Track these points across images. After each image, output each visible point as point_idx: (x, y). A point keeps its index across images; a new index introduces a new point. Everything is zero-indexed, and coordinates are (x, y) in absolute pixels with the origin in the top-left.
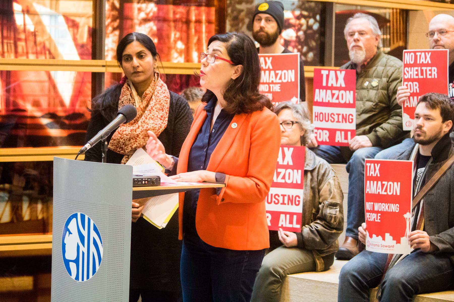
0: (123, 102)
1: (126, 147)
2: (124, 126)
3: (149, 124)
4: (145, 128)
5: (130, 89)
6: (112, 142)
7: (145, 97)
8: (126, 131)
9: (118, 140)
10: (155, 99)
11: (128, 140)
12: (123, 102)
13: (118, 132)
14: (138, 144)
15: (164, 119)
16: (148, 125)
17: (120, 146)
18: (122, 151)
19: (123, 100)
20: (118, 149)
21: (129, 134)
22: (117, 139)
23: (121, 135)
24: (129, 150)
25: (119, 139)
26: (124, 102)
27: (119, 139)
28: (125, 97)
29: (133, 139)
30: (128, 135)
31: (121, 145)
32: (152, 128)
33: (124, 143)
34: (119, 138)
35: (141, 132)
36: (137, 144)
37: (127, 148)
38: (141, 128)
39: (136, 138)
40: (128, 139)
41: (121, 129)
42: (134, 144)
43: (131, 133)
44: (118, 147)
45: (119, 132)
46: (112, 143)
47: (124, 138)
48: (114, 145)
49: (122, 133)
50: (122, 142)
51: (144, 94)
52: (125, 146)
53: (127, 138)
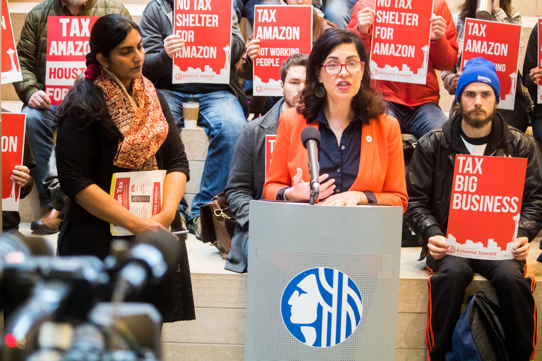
0: (115, 103)
1: (137, 160)
2: (130, 134)
3: (156, 128)
4: (155, 133)
5: (118, 87)
6: (122, 156)
7: (136, 94)
8: (136, 139)
9: (129, 152)
10: (150, 95)
11: (141, 150)
12: (115, 103)
13: (126, 142)
14: (152, 153)
15: (164, 119)
16: (156, 130)
17: (130, 159)
18: (132, 166)
19: (114, 101)
20: (127, 163)
21: (141, 142)
22: (128, 151)
23: (132, 145)
24: (143, 162)
25: (130, 151)
26: (116, 103)
27: (130, 151)
28: (116, 96)
29: (145, 149)
30: (140, 144)
31: (131, 158)
32: (161, 131)
33: (136, 154)
34: (130, 150)
35: (152, 138)
36: (151, 154)
37: (139, 160)
38: (150, 133)
39: (149, 146)
40: (140, 149)
41: (128, 138)
42: (148, 154)
43: (143, 141)
44: (128, 160)
45: (129, 142)
46: (122, 158)
47: (135, 149)
48: (124, 159)
49: (133, 143)
50: (133, 154)
51: (134, 91)
52: (136, 159)
53: (139, 148)
